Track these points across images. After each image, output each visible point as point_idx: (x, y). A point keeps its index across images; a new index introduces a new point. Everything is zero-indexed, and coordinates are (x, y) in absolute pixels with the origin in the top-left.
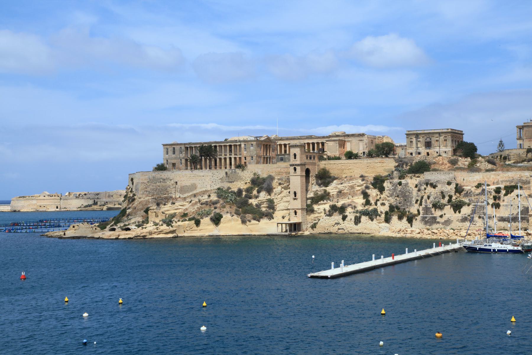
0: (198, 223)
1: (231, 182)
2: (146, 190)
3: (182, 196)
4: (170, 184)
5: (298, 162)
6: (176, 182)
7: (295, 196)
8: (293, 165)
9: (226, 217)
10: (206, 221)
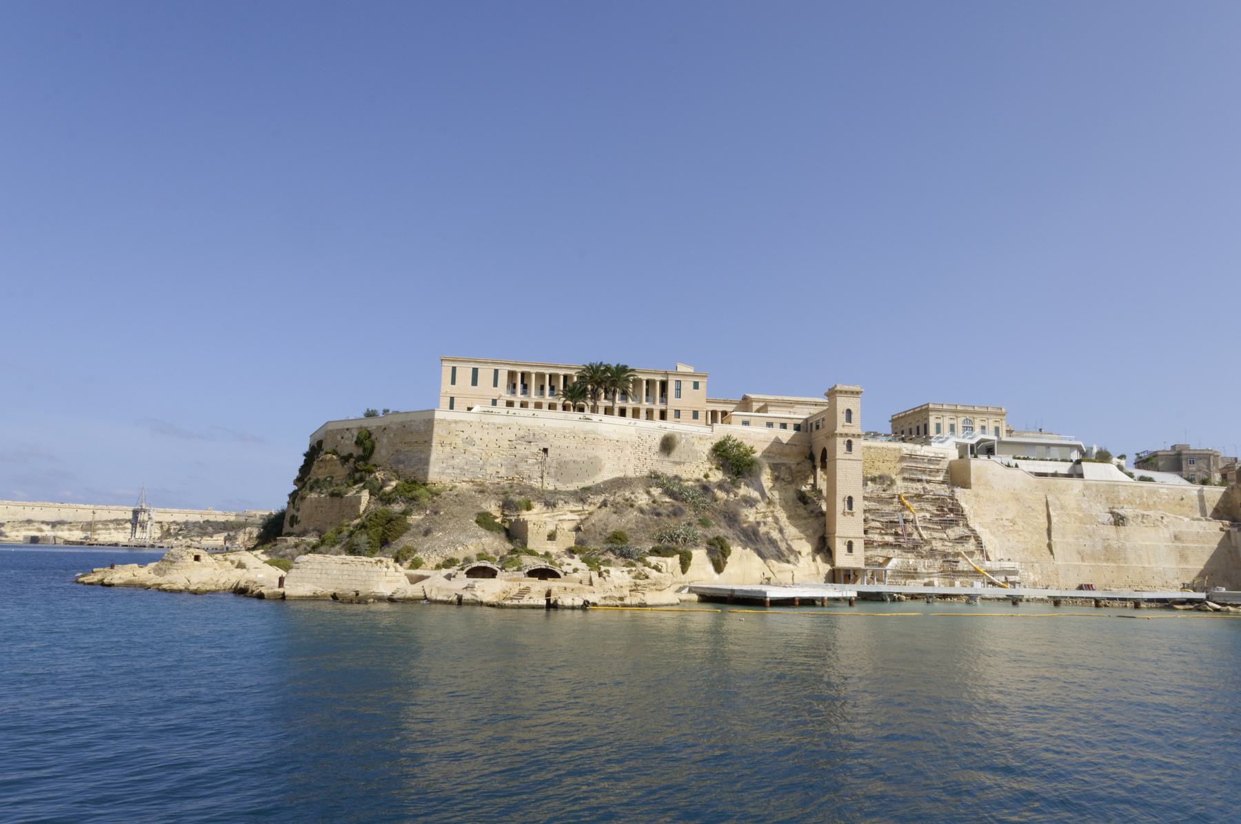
0: (685, 564)
1: (679, 463)
2: (451, 462)
3: (561, 487)
4: (527, 452)
5: (858, 431)
6: (545, 450)
7: (850, 507)
8: (847, 435)
9: (737, 551)
10: (699, 555)
